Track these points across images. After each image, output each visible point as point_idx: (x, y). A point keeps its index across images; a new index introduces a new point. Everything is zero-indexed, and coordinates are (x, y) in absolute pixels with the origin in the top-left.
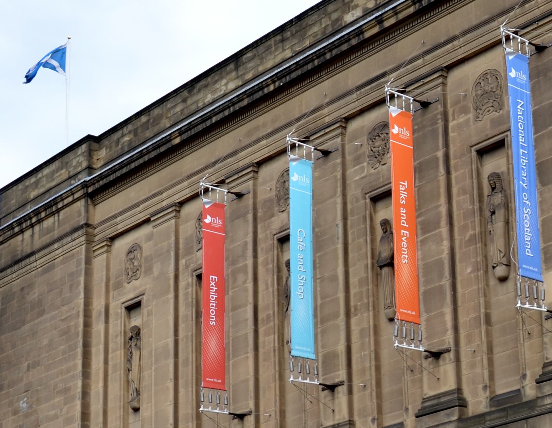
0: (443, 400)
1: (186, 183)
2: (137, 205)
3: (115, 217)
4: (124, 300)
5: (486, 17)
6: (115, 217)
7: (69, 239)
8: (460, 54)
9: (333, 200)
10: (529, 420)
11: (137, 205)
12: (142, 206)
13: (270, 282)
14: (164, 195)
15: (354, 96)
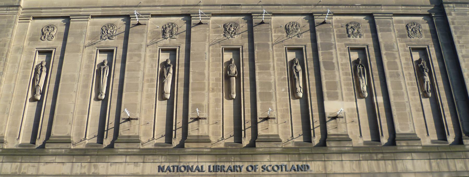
0: (271, 137)
1: (100, 9)
2: (61, 8)
3: (41, 9)
4: (38, 47)
5: (295, 3)
6: (41, 9)
7: (5, 9)
8: (282, 11)
9: (203, 43)
10: (326, 155)
11: (61, 8)
12: (63, 10)
13: (154, 65)
14: (82, 9)
15: (180, 8)
